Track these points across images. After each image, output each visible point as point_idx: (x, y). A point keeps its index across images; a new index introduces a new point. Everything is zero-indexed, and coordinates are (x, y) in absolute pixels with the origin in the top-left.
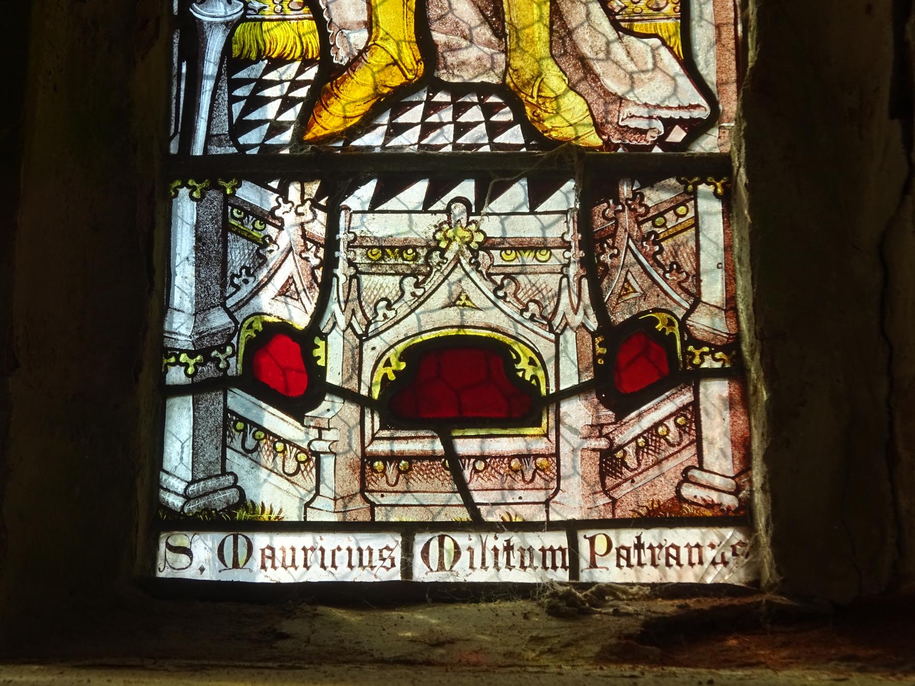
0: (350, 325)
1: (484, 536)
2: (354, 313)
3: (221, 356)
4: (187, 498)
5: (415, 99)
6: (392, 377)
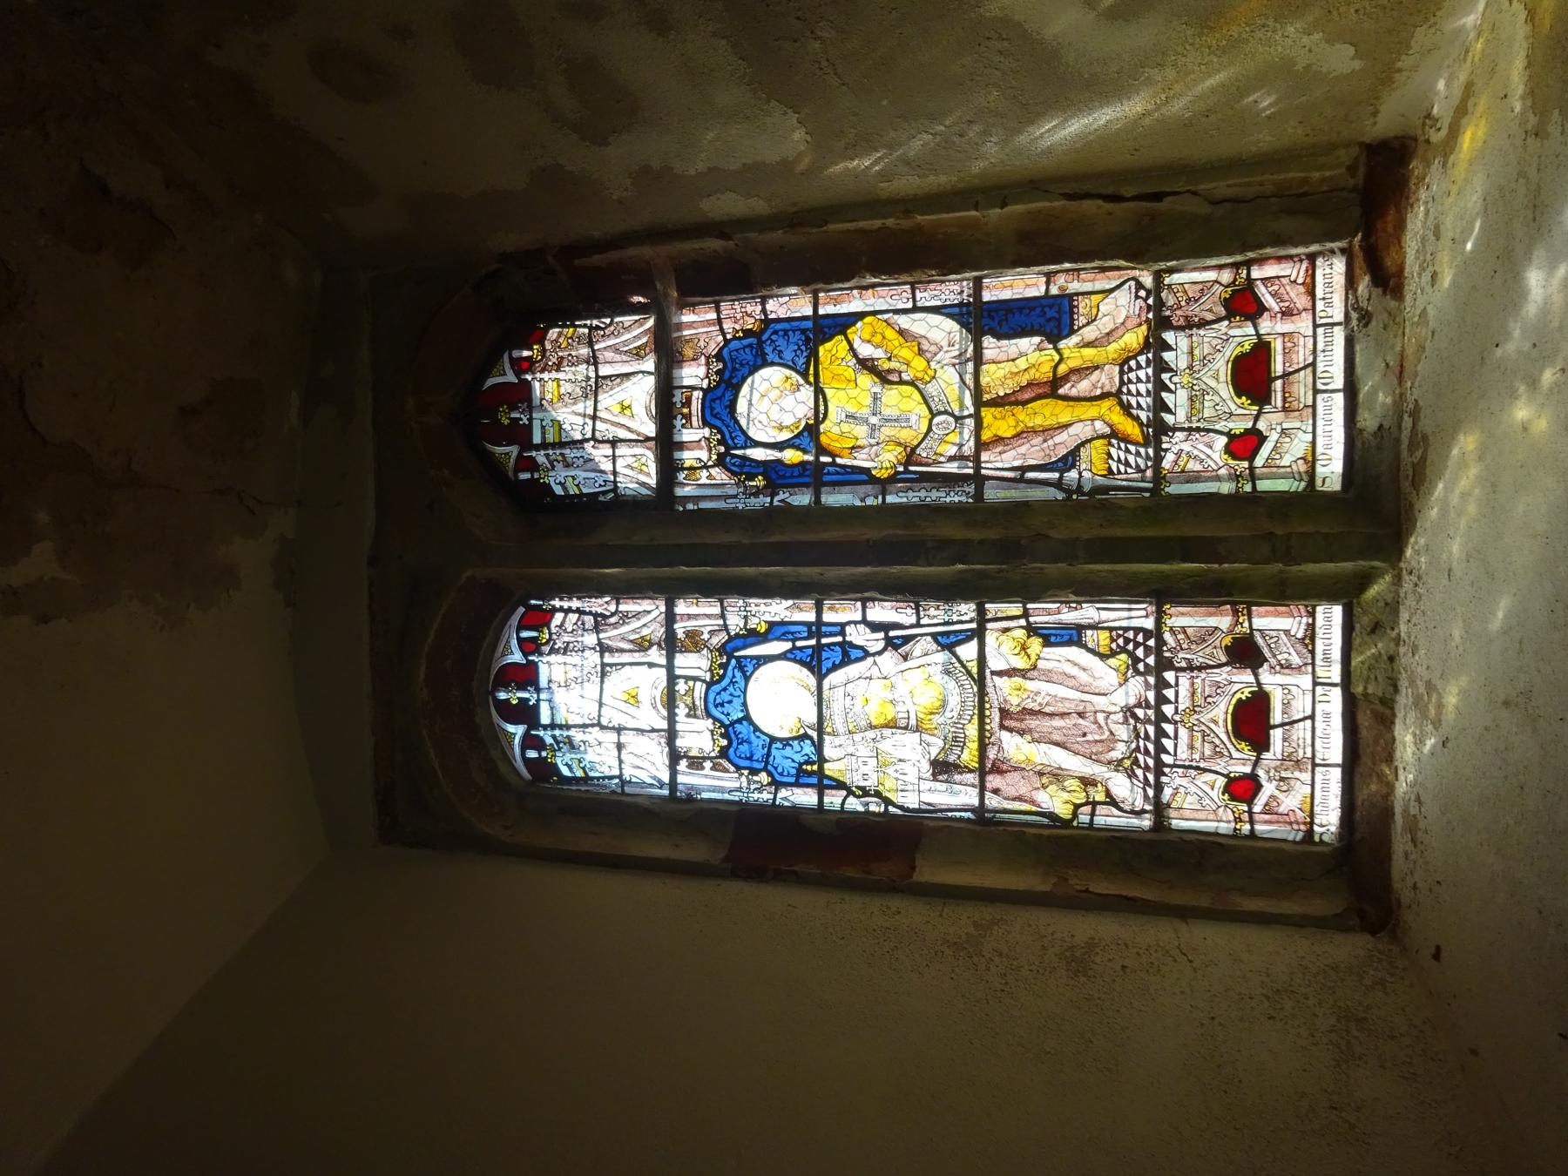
0: (1226, 420)
1: (1318, 361)
2: (1220, 418)
3: (1239, 470)
4: (1301, 480)
5: (1125, 402)
6: (1249, 402)
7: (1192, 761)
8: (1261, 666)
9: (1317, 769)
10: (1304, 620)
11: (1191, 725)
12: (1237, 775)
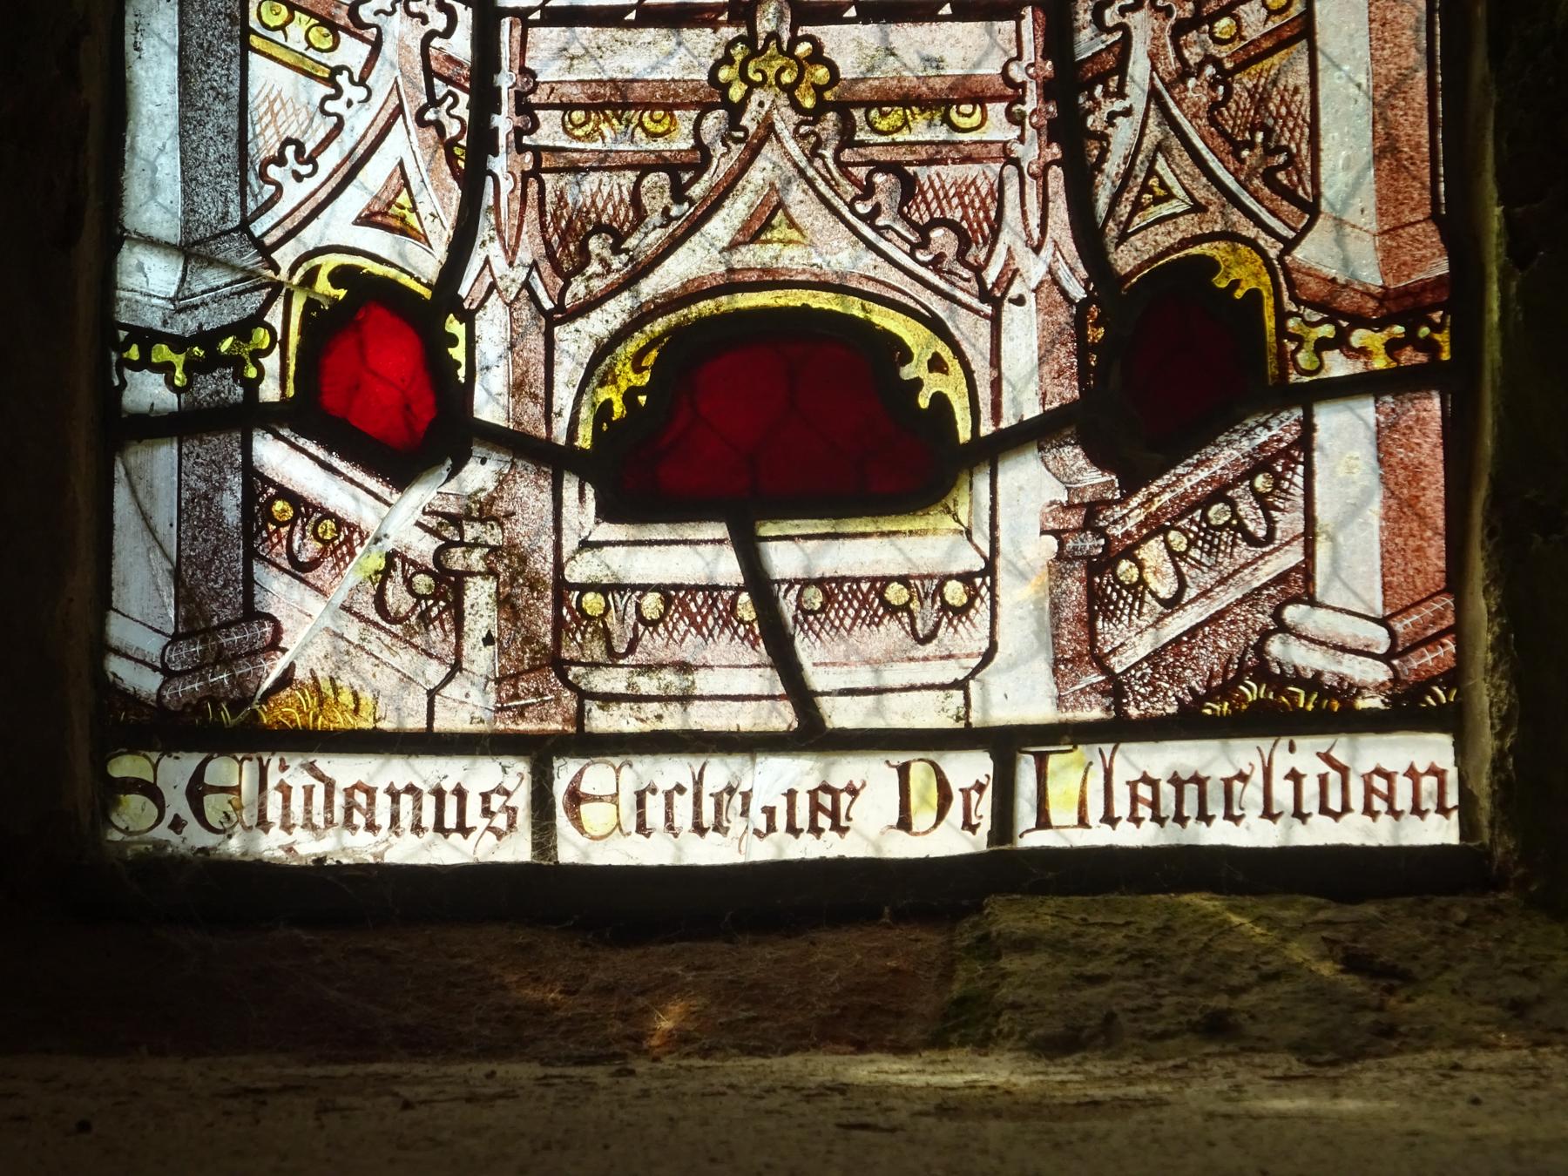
7: (524, 107)
8: (1098, 459)
9: (515, 774)
10: (1378, 673)
11: (736, 93)
12: (458, 353)
